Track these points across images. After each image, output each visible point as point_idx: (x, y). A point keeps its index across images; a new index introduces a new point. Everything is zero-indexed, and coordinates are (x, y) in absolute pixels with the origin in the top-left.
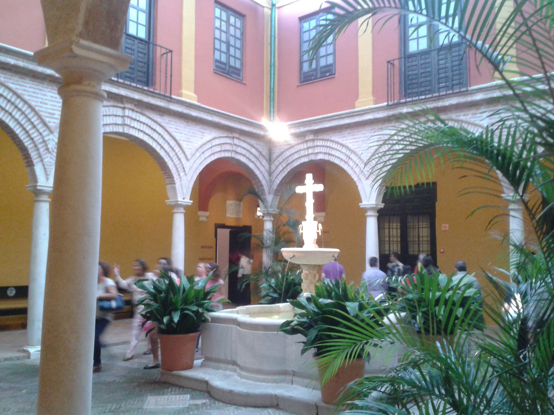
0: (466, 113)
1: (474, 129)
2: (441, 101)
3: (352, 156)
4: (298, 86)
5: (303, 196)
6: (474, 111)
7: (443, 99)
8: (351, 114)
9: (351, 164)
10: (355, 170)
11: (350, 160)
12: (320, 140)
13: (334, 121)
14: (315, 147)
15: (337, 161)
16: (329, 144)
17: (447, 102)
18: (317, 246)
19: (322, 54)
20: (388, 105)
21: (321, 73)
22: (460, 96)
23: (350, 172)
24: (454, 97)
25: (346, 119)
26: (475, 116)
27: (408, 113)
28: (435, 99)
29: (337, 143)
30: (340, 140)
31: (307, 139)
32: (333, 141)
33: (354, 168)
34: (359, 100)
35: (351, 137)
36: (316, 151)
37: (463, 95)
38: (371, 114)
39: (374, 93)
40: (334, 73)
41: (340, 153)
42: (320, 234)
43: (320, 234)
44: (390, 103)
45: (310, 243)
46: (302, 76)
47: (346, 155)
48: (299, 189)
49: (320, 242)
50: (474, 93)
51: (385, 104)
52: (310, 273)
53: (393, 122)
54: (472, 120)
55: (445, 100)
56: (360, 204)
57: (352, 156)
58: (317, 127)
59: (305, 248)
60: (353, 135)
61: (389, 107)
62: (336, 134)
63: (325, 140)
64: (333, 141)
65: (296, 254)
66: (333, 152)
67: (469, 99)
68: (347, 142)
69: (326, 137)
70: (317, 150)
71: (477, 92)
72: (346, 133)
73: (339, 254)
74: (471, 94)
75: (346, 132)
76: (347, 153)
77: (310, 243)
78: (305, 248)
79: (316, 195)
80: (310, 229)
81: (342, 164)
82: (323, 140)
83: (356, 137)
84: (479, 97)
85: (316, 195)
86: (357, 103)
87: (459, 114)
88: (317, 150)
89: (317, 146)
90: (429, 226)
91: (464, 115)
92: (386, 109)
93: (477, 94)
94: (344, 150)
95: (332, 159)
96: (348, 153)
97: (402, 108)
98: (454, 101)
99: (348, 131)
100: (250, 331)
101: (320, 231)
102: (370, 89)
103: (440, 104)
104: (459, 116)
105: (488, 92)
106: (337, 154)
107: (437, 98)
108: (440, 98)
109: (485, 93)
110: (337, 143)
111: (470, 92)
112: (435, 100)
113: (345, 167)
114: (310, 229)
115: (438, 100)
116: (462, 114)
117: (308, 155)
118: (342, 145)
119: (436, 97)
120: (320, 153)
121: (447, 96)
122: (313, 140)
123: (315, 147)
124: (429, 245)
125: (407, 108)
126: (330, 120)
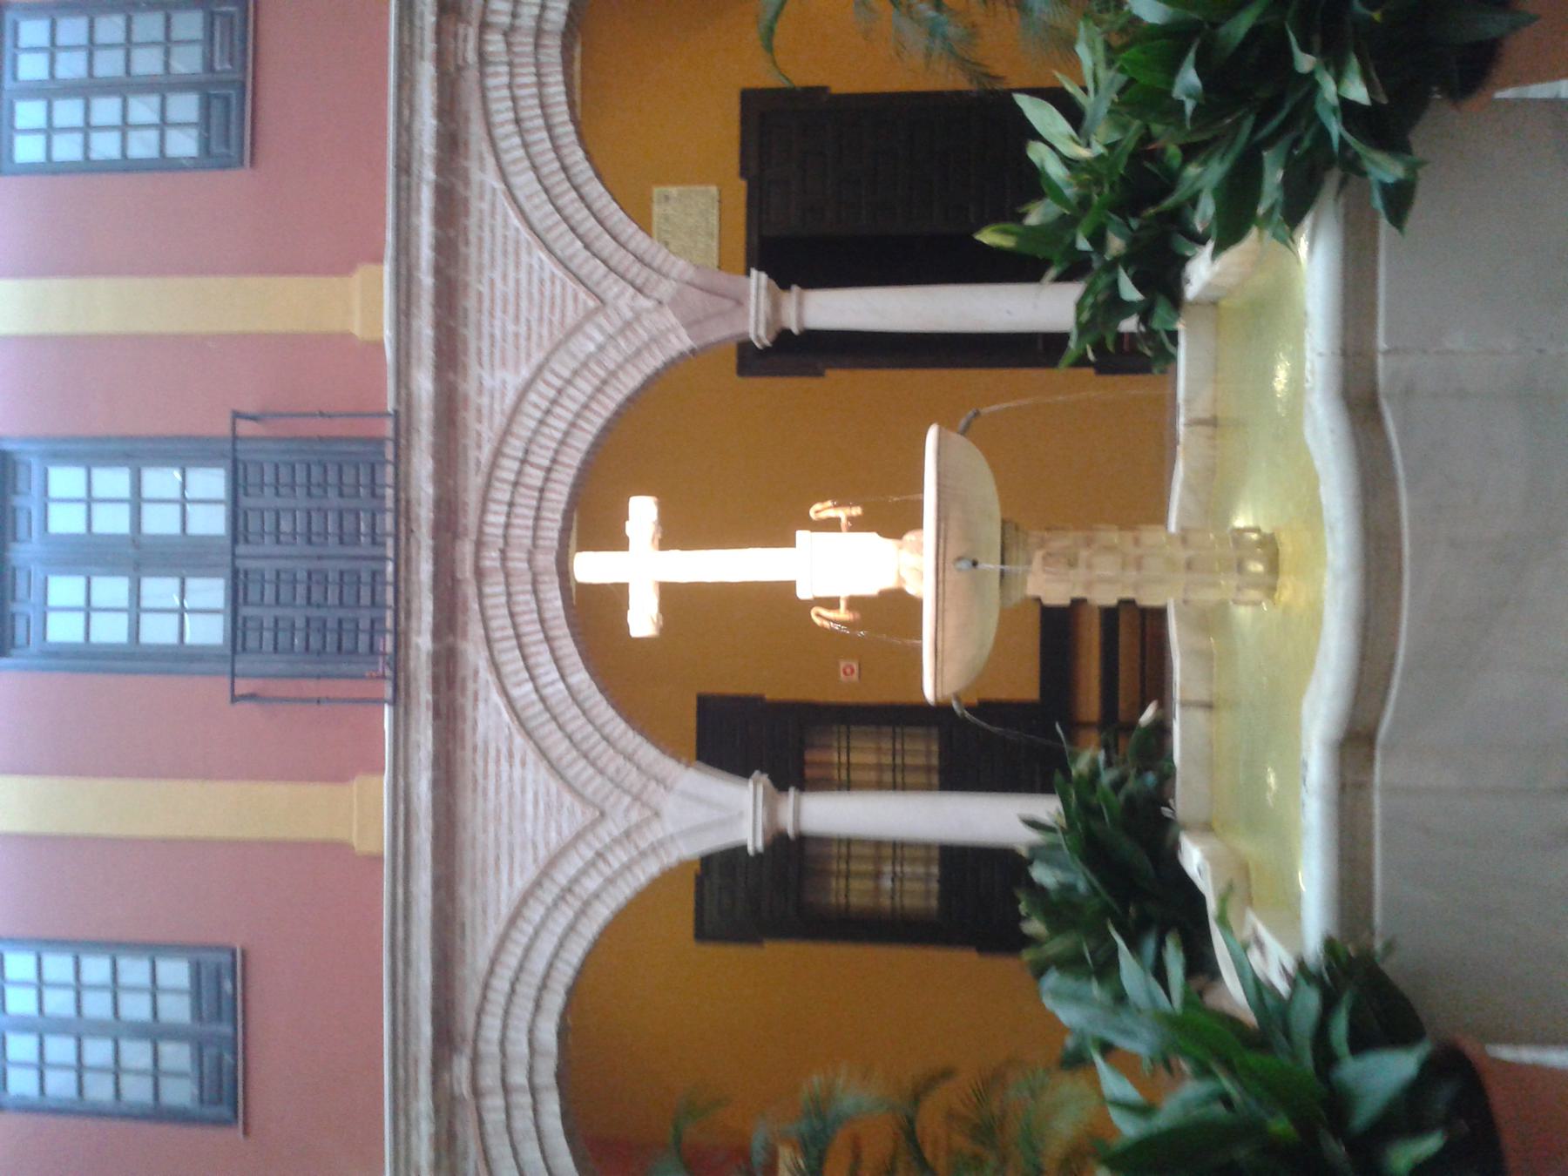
0: (471, 442)
1: (530, 416)
2: (415, 508)
3: (562, 876)
4: (246, 1132)
5: (671, 595)
6: (470, 416)
7: (408, 502)
8: (400, 860)
9: (591, 883)
10: (616, 865)
11: (577, 889)
12: (478, 1024)
13: (414, 945)
14: (504, 1053)
15: (576, 952)
16: (501, 984)
17: (424, 490)
18: (910, 537)
19: (123, 963)
20: (394, 702)
21: (218, 1017)
22: (409, 446)
23: (623, 892)
24: (409, 461)
25: (414, 889)
26: (485, 411)
27: (437, 634)
28: (402, 527)
29: (503, 940)
30: (495, 929)
31: (464, 1088)
32: (494, 962)
33: (607, 871)
34: (355, 841)
35: (491, 880)
36: (525, 1049)
37: (408, 431)
38: (413, 778)
39: (339, 776)
40: (225, 958)
41: (544, 935)
42: (856, 511)
43: (856, 511)
44: (388, 692)
45: (903, 564)
46: (211, 1111)
47: (555, 904)
48: (643, 620)
49: (892, 517)
50: (409, 394)
51: (387, 710)
52: (1042, 544)
53: (460, 700)
54: (499, 421)
55: (413, 494)
56: (750, 849)
57: (562, 876)
58: (426, 1029)
59: (923, 587)
60: (484, 872)
61: (401, 698)
62: (468, 949)
63: (484, 997)
64: (494, 962)
65: (954, 550)
66: (538, 965)
67: (425, 415)
68: (503, 897)
69: (470, 998)
70: (519, 1047)
71: (408, 388)
72: (468, 902)
73: (947, 424)
74: (409, 407)
75: (468, 899)
76: (549, 899)
77: (903, 564)
78: (923, 587)
79: (673, 535)
80: (835, 565)
81: (590, 929)
82: (480, 1012)
83: (491, 860)
84: (424, 383)
85: (673, 535)
86: (363, 846)
87: (472, 464)
88: (519, 1047)
89: (503, 1042)
90: (843, 728)
91: (479, 447)
92: (407, 713)
93: (414, 387)
94: (535, 912)
95: (565, 974)
96: (549, 893)
97: (413, 653)
98: (423, 466)
99: (464, 890)
100: (1407, 577)
101: (842, 514)
102: (317, 792)
103: (424, 514)
104: (478, 463)
105: (414, 353)
106: (546, 946)
107: (402, 520)
108: (403, 511)
109: (414, 361)
110: (503, 940)
111: (402, 410)
112: (410, 531)
113: (602, 913)
114: (835, 565)
115: (408, 519)
116: (472, 454)
117: (533, 1091)
118: (513, 921)
119: (397, 524)
120: (531, 1031)
121: (401, 483)
122: (475, 1060)
123: (504, 1053)
124: (908, 730)
125: (419, 633)
126: (407, 963)
